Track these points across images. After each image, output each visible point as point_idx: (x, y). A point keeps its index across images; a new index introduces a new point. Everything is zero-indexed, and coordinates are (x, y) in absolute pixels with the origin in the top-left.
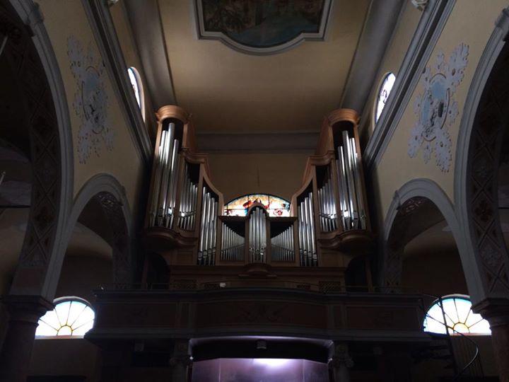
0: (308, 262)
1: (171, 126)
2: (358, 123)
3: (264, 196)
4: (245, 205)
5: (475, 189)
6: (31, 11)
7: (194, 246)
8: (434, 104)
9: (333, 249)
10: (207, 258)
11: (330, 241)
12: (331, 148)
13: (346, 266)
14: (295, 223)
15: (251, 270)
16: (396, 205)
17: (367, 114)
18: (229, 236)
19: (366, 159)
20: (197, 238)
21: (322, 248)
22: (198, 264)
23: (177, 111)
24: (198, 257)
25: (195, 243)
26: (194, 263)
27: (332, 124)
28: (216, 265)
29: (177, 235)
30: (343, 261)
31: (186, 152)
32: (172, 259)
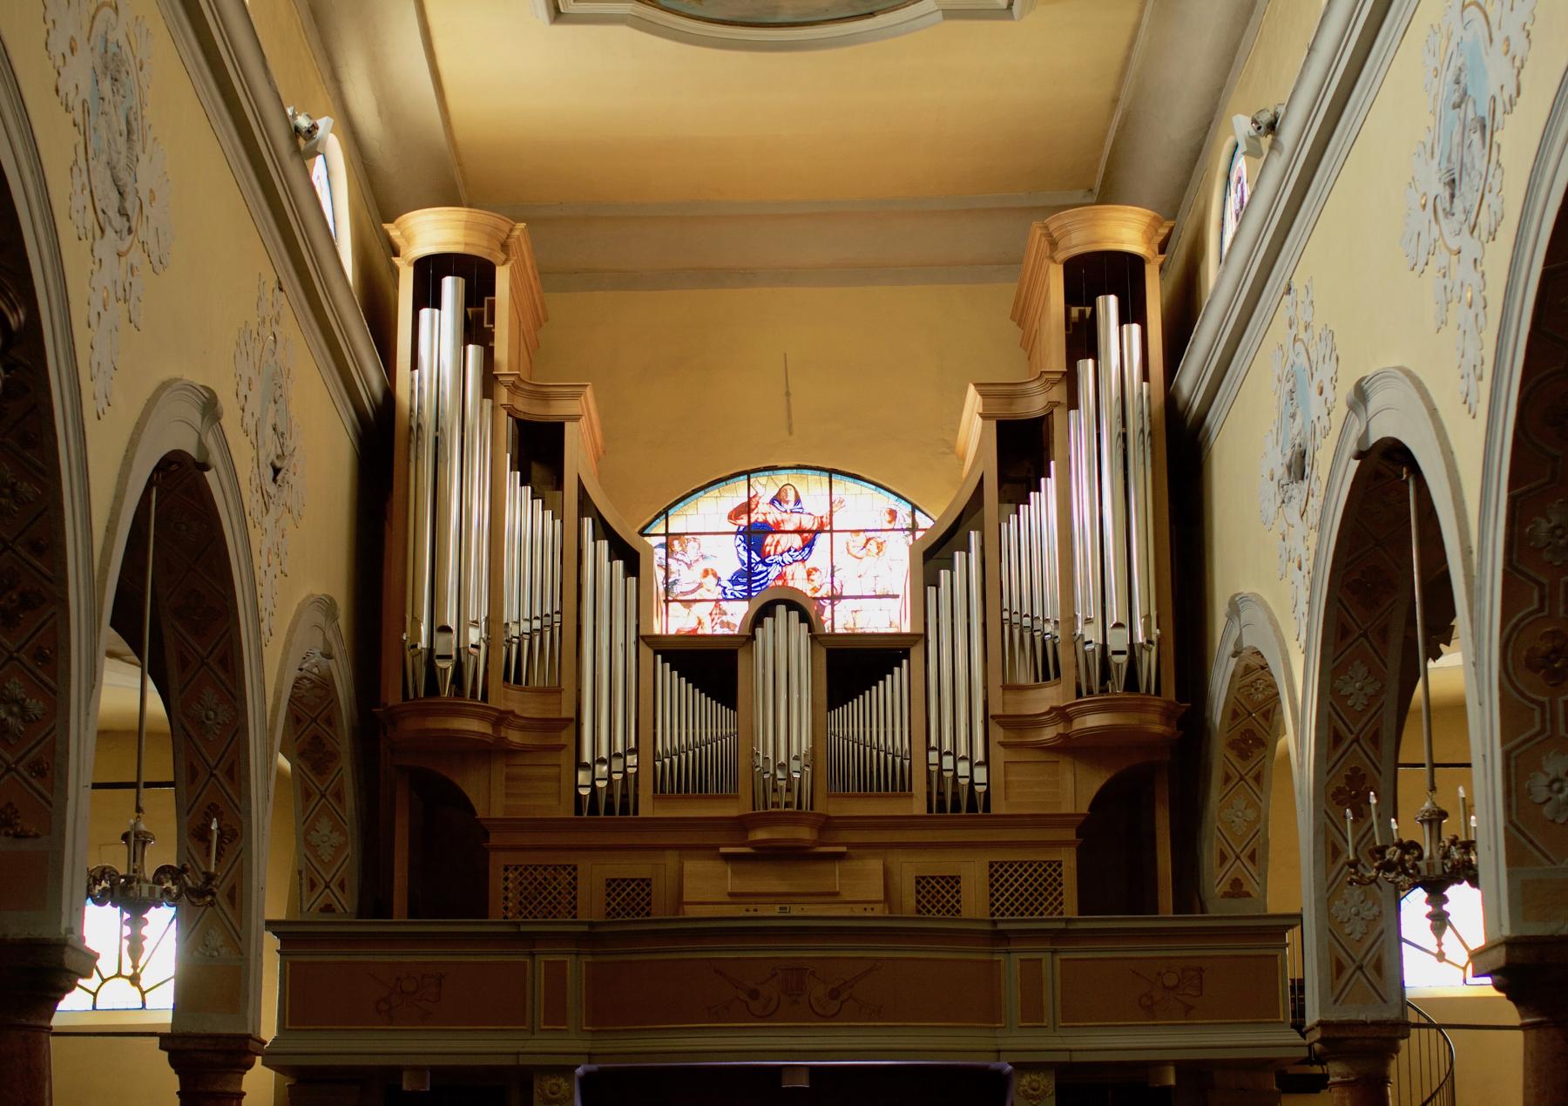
0: (955, 794)
1: (450, 287)
2: (1163, 248)
3: (813, 477)
4: (734, 515)
5: (1337, 739)
6: (203, 416)
7: (560, 748)
8: (1314, 391)
9: (1040, 747)
10: (610, 796)
11: (1034, 722)
12: (1056, 360)
13: (1084, 809)
14: (916, 653)
15: (761, 835)
16: (1351, 447)
17: (1202, 203)
18: (684, 717)
19: (1180, 405)
20: (570, 720)
21: (1003, 744)
22: (578, 811)
23: (470, 226)
24: (577, 786)
25: (566, 737)
26: (566, 811)
27: (1062, 255)
28: (642, 814)
29: (502, 718)
30: (1074, 790)
31: (514, 389)
32: (489, 795)
